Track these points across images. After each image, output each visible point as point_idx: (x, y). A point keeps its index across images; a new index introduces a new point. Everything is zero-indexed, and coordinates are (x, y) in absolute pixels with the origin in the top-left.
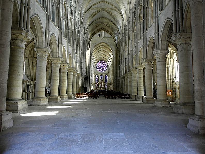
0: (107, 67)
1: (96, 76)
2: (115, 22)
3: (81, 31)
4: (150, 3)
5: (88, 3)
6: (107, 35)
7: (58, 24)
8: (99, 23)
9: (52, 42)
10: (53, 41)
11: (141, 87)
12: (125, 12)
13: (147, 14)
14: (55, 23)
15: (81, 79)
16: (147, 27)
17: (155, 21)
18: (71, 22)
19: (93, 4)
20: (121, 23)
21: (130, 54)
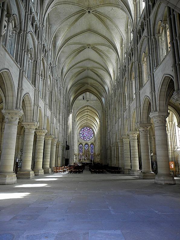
0: (93, 135)
2: (101, 82)
3: (62, 92)
4: (142, 59)
5: (71, 60)
6: (93, 97)
7: (34, 83)
8: (83, 84)
10: (27, 102)
11: (135, 159)
13: (139, 72)
14: (31, 81)
15: (62, 149)
17: (150, 78)
18: (50, 82)
19: (76, 62)
20: (109, 83)
21: (120, 119)
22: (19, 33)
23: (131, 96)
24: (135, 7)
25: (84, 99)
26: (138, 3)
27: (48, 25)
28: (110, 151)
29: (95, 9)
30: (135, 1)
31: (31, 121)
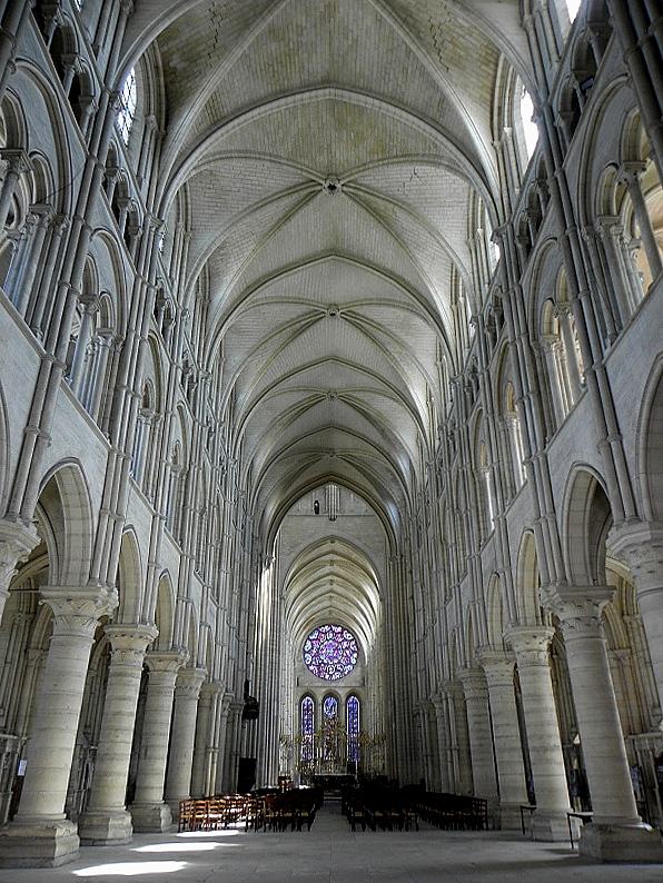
0: (355, 655)
1: (305, 701)
3: (231, 479)
4: (545, 327)
5: (268, 363)
6: (354, 503)
7: (108, 423)
8: (316, 453)
9: (67, 506)
10: (68, 498)
11: (549, 755)
12: (429, 397)
13: (536, 376)
14: (96, 417)
15: (226, 713)
16: (545, 431)
18: (184, 433)
20: (411, 443)
21: (468, 576)
22: (55, 224)
23: (508, 480)
24: (500, 155)
25: (317, 510)
26: (510, 142)
27: (181, 230)
28: (429, 722)
29: (352, 178)
30: (496, 138)
31: (80, 581)
